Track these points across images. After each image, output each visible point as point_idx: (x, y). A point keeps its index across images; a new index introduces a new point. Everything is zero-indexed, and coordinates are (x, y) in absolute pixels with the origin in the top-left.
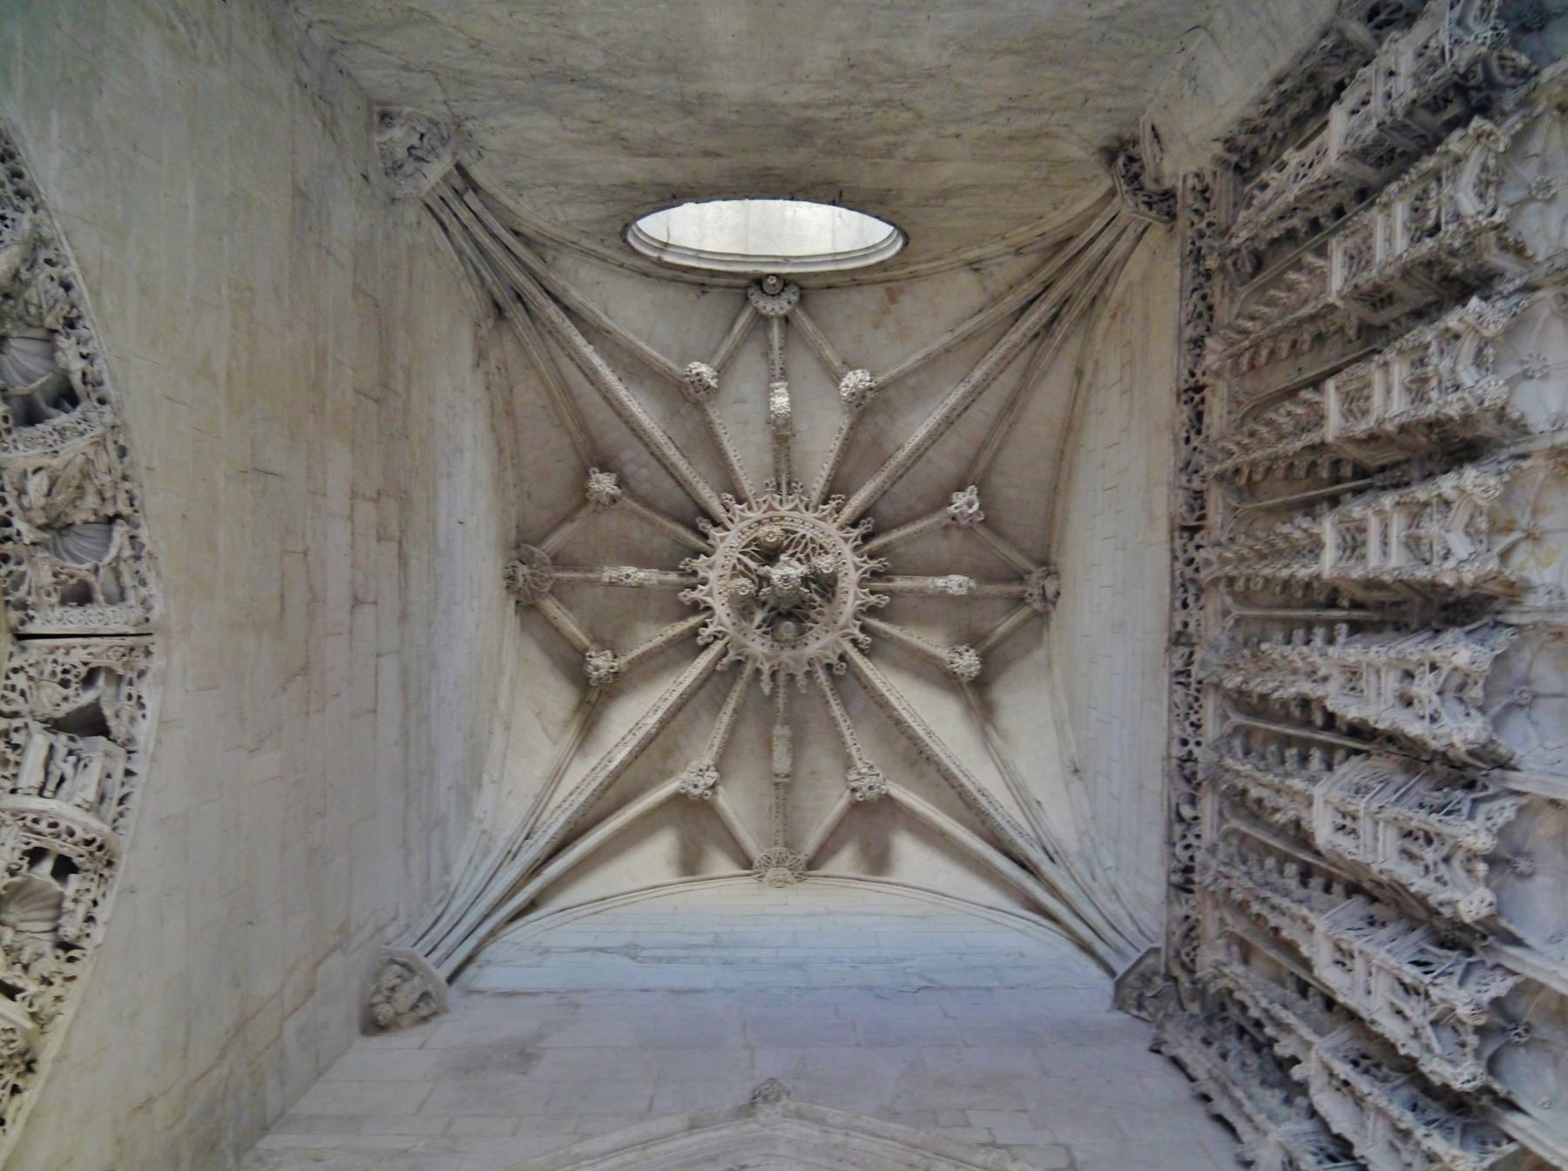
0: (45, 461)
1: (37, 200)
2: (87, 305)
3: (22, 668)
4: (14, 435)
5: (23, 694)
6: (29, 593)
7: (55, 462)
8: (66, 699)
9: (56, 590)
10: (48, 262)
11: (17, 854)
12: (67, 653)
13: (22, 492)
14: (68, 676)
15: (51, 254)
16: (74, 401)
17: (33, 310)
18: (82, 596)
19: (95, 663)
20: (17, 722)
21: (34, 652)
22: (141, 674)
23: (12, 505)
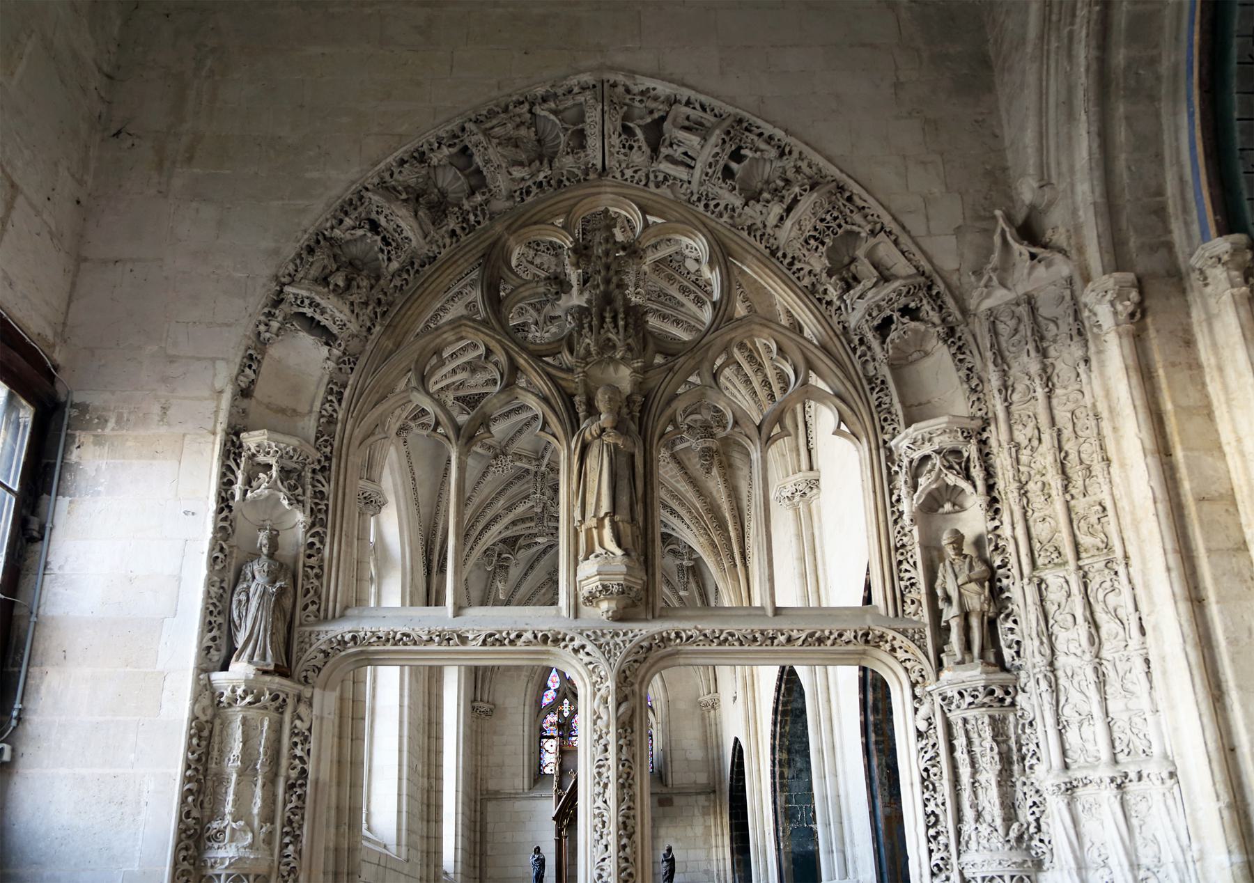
0: (504, 170)
1: (360, 188)
2: (409, 147)
3: (621, 171)
4: (492, 187)
5: (635, 172)
6: (579, 168)
7: (504, 165)
8: (640, 148)
9: (577, 153)
10: (392, 175)
11: (723, 185)
12: (613, 146)
13: (523, 179)
14: (627, 145)
15: (387, 176)
16: (466, 148)
17: (421, 180)
18: (580, 137)
19: (619, 129)
20: (652, 177)
21: (612, 163)
22: (628, 91)
23: (530, 183)
